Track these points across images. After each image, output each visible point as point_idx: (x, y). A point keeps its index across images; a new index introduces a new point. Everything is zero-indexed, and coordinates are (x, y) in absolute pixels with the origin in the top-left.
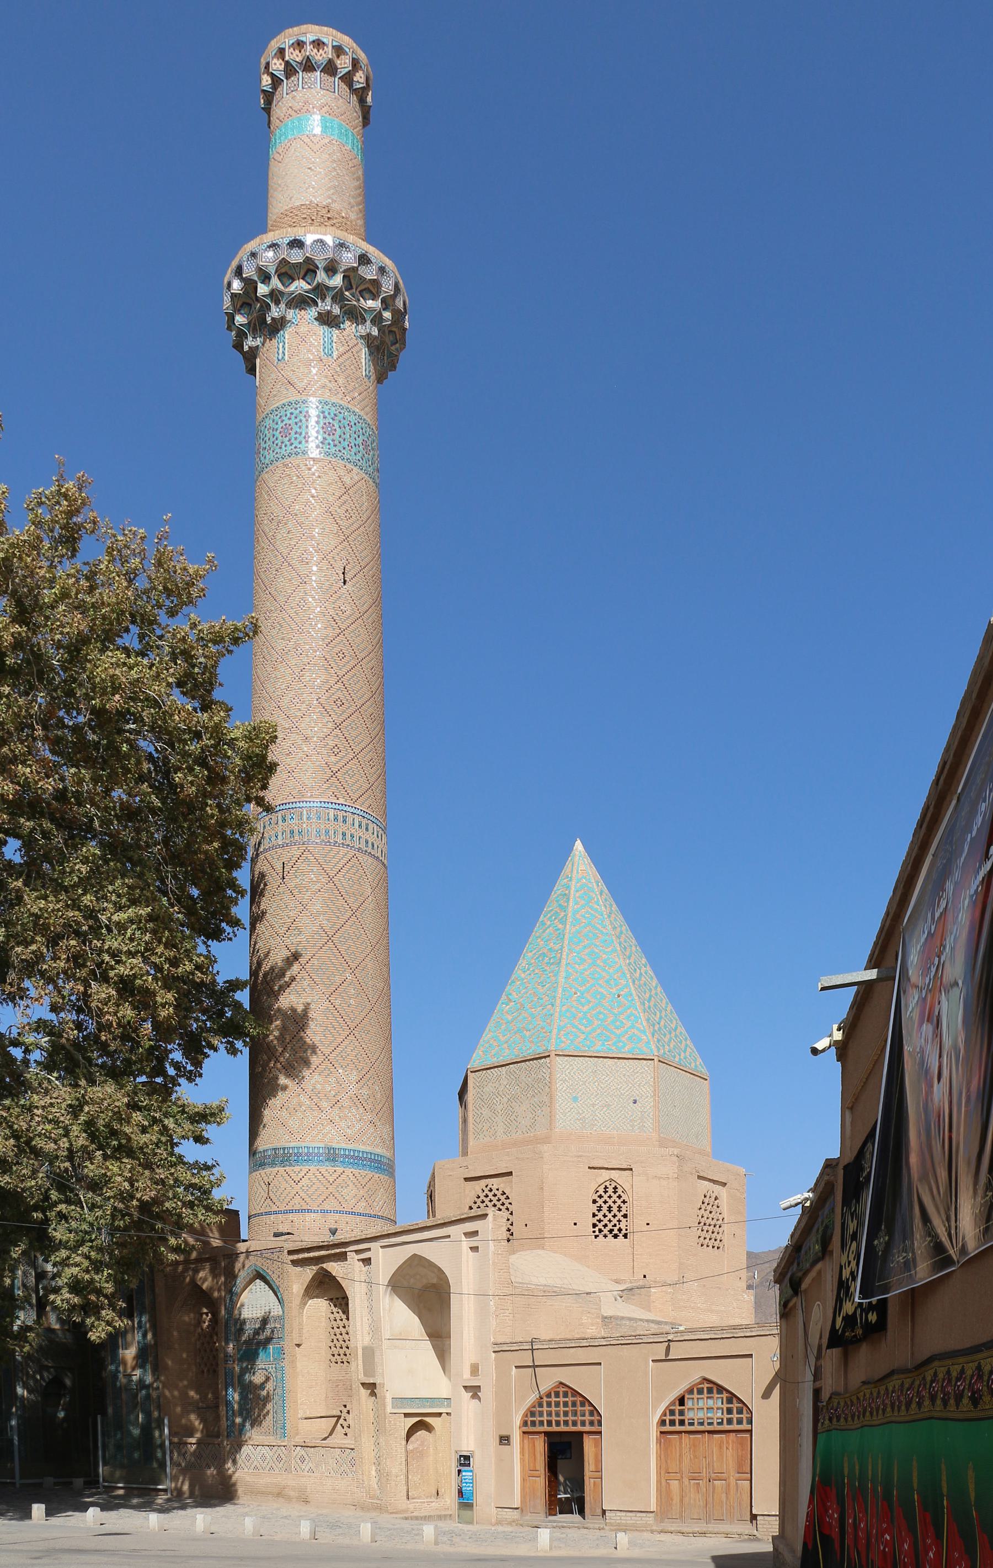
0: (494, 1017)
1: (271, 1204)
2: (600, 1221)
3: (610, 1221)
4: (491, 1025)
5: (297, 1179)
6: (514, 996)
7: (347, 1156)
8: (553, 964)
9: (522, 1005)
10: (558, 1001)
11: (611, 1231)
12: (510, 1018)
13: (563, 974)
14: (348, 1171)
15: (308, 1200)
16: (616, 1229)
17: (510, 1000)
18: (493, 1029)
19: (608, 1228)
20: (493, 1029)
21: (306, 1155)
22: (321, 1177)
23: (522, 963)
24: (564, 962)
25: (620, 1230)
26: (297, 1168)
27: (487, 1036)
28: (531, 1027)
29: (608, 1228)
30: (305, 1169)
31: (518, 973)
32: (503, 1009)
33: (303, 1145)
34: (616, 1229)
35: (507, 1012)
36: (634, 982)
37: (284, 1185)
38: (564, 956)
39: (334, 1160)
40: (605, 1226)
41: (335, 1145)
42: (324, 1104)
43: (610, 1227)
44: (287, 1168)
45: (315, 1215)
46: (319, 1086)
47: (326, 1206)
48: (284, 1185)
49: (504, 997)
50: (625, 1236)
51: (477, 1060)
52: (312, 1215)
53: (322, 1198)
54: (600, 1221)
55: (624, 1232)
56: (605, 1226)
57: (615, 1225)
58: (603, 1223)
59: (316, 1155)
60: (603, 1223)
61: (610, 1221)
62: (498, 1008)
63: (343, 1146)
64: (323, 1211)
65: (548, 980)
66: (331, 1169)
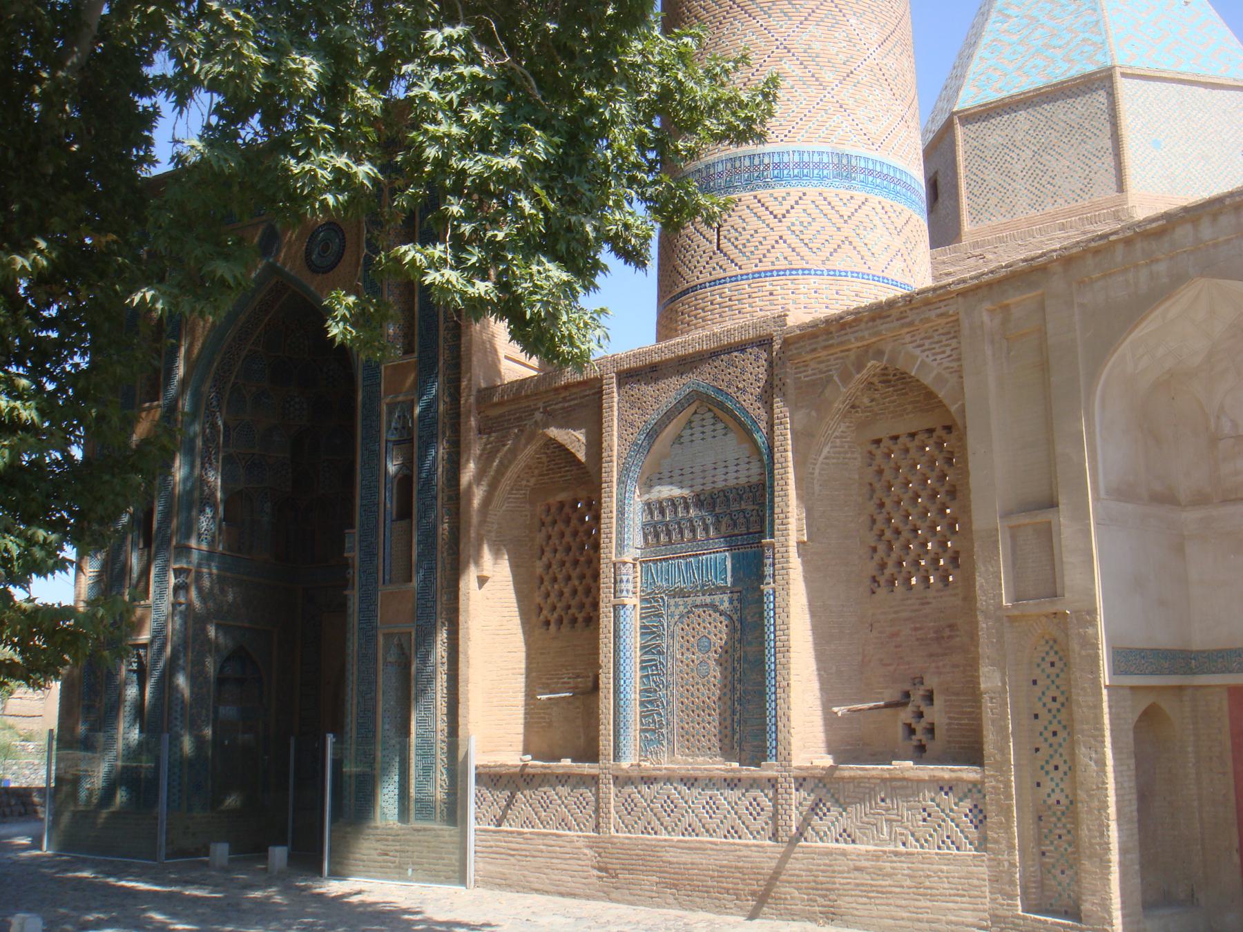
1: (724, 262)
5: (779, 211)
7: (871, 172)
14: (875, 199)
15: (804, 251)
21: (797, 165)
22: (827, 209)
26: (779, 191)
30: (795, 192)
33: (791, 147)
37: (754, 223)
39: (848, 177)
41: (848, 149)
42: (828, 76)
44: (761, 193)
45: (816, 279)
46: (817, 46)
47: (838, 263)
48: (754, 223)
52: (812, 279)
53: (829, 248)
59: (817, 165)
63: (863, 152)
64: (833, 273)
66: (845, 194)
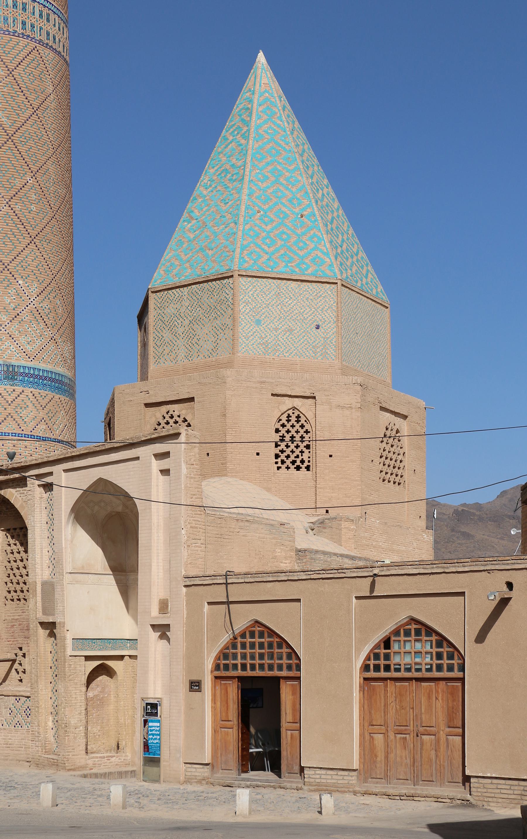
0: (176, 235)
2: (282, 451)
3: (292, 452)
4: (172, 244)
6: (196, 214)
8: (235, 181)
9: (204, 223)
10: (241, 219)
11: (293, 462)
12: (192, 236)
13: (246, 191)
16: (298, 460)
17: (192, 218)
18: (174, 247)
19: (290, 460)
20: (174, 247)
23: (204, 179)
24: (247, 179)
25: (302, 462)
27: (168, 255)
28: (213, 246)
29: (290, 460)
31: (200, 190)
32: (185, 228)
34: (298, 460)
35: (189, 231)
36: (317, 202)
38: (247, 173)
40: (288, 457)
43: (292, 458)
49: (185, 215)
50: (308, 468)
51: (158, 280)
54: (282, 451)
55: (306, 464)
56: (288, 457)
57: (297, 457)
58: (285, 454)
60: (285, 454)
61: (292, 452)
62: (179, 225)
65: (231, 198)
